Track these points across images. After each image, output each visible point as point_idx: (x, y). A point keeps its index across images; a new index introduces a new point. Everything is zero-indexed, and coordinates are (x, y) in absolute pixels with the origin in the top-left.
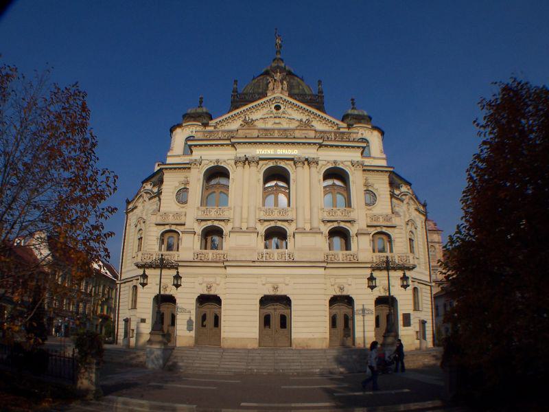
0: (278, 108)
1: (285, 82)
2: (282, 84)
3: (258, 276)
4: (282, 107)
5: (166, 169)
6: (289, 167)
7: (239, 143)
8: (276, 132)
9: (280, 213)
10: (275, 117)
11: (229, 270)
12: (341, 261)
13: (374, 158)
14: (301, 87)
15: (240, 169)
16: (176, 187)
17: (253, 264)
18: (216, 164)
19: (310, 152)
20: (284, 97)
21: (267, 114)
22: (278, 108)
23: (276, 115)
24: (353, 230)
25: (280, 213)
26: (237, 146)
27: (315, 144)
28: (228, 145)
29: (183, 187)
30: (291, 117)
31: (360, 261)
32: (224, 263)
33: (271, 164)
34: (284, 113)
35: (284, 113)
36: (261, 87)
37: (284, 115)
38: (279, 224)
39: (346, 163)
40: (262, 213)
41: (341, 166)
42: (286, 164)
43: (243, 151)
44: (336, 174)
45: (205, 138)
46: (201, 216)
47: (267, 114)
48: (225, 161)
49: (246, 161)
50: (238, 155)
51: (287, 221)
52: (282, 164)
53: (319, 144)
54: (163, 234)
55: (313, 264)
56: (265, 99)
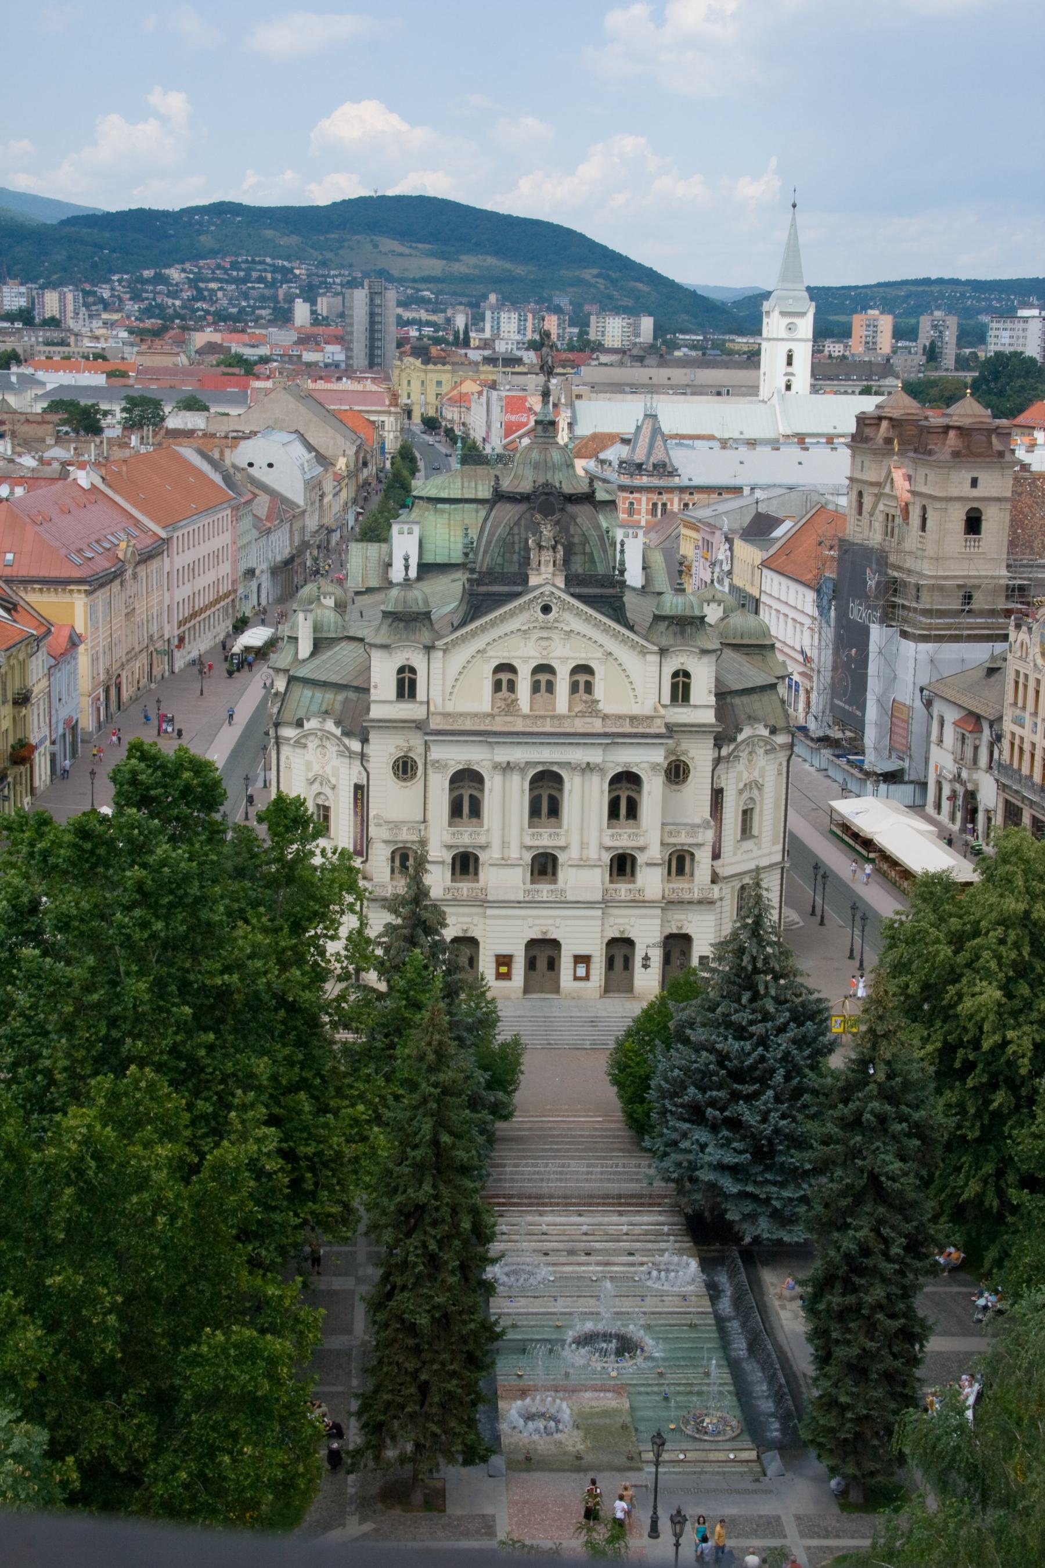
0: (546, 609)
1: (559, 547)
3: (524, 918)
4: (555, 609)
6: (563, 773)
11: (489, 912)
12: (623, 898)
13: (695, 706)
14: (588, 550)
15: (498, 779)
17: (519, 904)
19: (594, 756)
21: (529, 621)
22: (546, 609)
24: (641, 859)
31: (647, 898)
32: (483, 903)
35: (556, 621)
39: (643, 765)
41: (634, 770)
43: (505, 754)
44: (627, 781)
46: (448, 839)
47: (529, 621)
49: (508, 768)
51: (560, 848)
52: (555, 769)
54: (393, 852)
55: (590, 904)
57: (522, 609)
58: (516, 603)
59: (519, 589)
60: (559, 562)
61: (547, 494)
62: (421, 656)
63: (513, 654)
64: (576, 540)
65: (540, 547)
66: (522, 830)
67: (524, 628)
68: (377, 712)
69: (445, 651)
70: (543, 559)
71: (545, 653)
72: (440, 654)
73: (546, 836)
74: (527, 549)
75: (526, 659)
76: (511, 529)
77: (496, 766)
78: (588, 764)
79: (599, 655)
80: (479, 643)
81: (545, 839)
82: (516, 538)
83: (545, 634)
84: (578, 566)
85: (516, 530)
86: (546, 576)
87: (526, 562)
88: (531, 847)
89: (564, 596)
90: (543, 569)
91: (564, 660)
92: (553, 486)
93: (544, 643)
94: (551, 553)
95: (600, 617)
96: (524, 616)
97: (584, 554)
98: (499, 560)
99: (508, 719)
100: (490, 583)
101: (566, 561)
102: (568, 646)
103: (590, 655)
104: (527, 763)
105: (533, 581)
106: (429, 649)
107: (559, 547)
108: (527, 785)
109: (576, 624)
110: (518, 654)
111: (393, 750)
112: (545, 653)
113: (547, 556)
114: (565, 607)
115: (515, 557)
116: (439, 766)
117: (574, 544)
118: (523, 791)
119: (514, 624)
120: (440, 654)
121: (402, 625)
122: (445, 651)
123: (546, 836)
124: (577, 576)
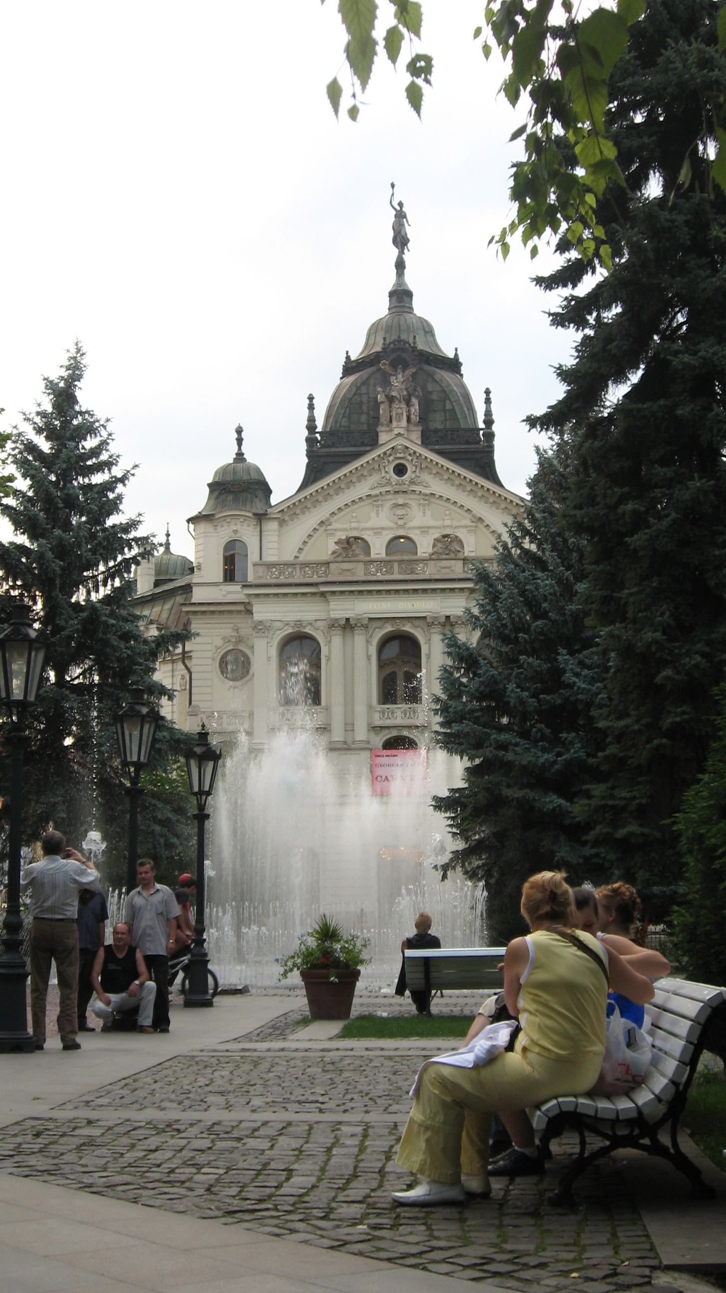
0: (400, 470)
1: (415, 401)
2: (408, 403)
5: (195, 612)
7: (333, 593)
8: (396, 565)
9: (405, 713)
10: (396, 492)
14: (448, 406)
15: (337, 640)
16: (217, 648)
18: (296, 629)
20: (414, 447)
22: (400, 470)
23: (397, 488)
25: (405, 715)
26: (330, 598)
27: (461, 589)
28: (314, 594)
29: (231, 648)
30: (427, 491)
33: (389, 628)
34: (412, 482)
36: (365, 408)
37: (414, 488)
38: (405, 733)
40: (377, 716)
42: (415, 627)
43: (342, 609)
45: (274, 581)
48: (310, 624)
49: (348, 626)
50: (335, 615)
52: (408, 628)
53: (469, 588)
56: (374, 454)
57: (372, 468)
58: (363, 460)
59: (368, 448)
60: (415, 418)
61: (399, 349)
62: (251, 528)
63: (363, 525)
64: (435, 397)
65: (391, 400)
66: (370, 707)
67: (373, 493)
68: (198, 595)
69: (282, 523)
70: (394, 414)
71: (401, 522)
72: (274, 525)
73: (399, 714)
74: (377, 405)
75: (378, 531)
76: (358, 388)
77: (333, 625)
78: (448, 617)
79: (467, 522)
80: (322, 512)
81: (398, 715)
82: (365, 398)
83: (400, 501)
84: (437, 422)
85: (364, 390)
86: (399, 435)
87: (376, 420)
88: (382, 728)
89: (421, 450)
90: (394, 424)
91: (425, 530)
92: (405, 342)
93: (400, 512)
94: (403, 406)
95: (464, 472)
96: (374, 479)
97: (445, 411)
98: (345, 422)
99: (346, 566)
100: (333, 445)
101: (423, 419)
102: (428, 513)
103: (456, 523)
104: (370, 619)
105: (383, 438)
106: (260, 518)
107: (415, 401)
108: (373, 650)
109: (438, 487)
110: (369, 524)
111: (218, 642)
112: (401, 522)
113: (400, 408)
114: (424, 465)
115: (364, 418)
116: (261, 628)
117: (432, 401)
118: (369, 658)
119: (363, 489)
120: (274, 525)
121: (230, 497)
122: (282, 523)
123: (399, 714)
124: (436, 431)
